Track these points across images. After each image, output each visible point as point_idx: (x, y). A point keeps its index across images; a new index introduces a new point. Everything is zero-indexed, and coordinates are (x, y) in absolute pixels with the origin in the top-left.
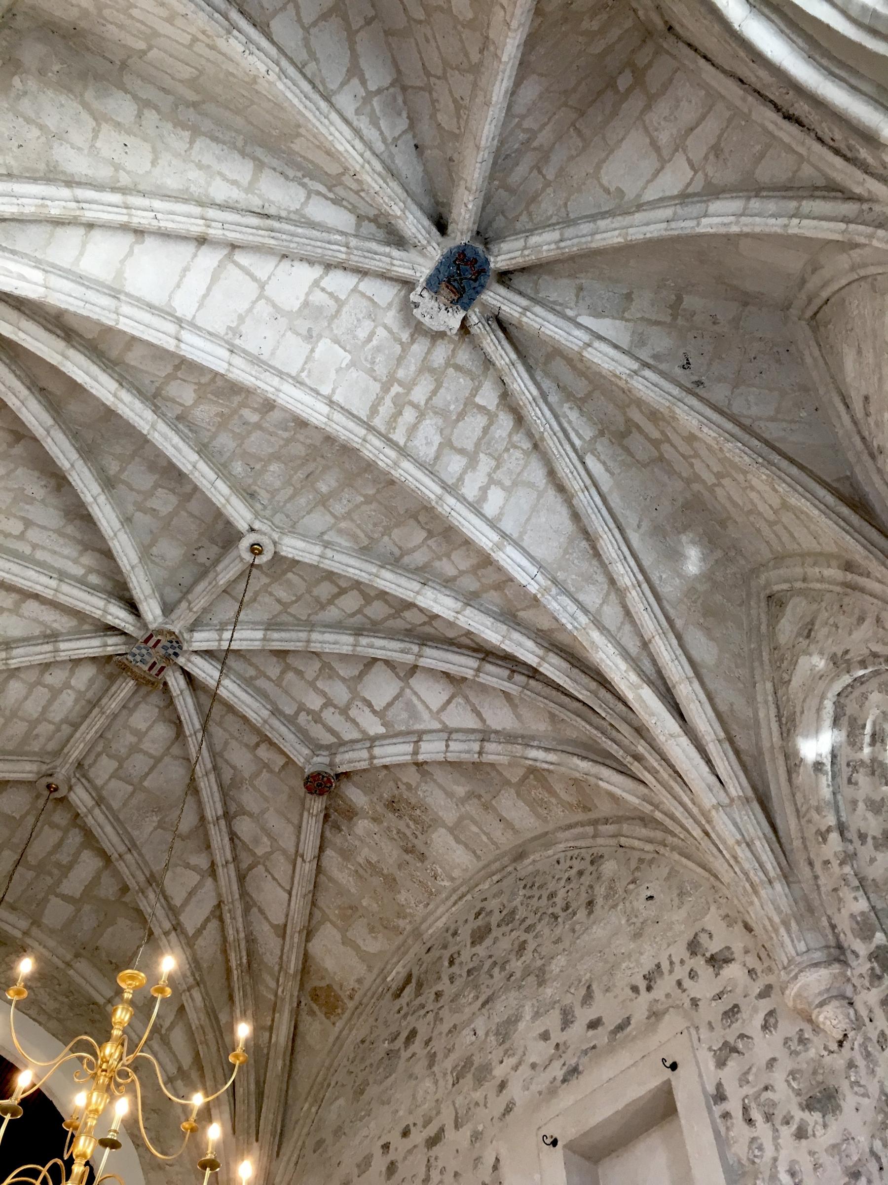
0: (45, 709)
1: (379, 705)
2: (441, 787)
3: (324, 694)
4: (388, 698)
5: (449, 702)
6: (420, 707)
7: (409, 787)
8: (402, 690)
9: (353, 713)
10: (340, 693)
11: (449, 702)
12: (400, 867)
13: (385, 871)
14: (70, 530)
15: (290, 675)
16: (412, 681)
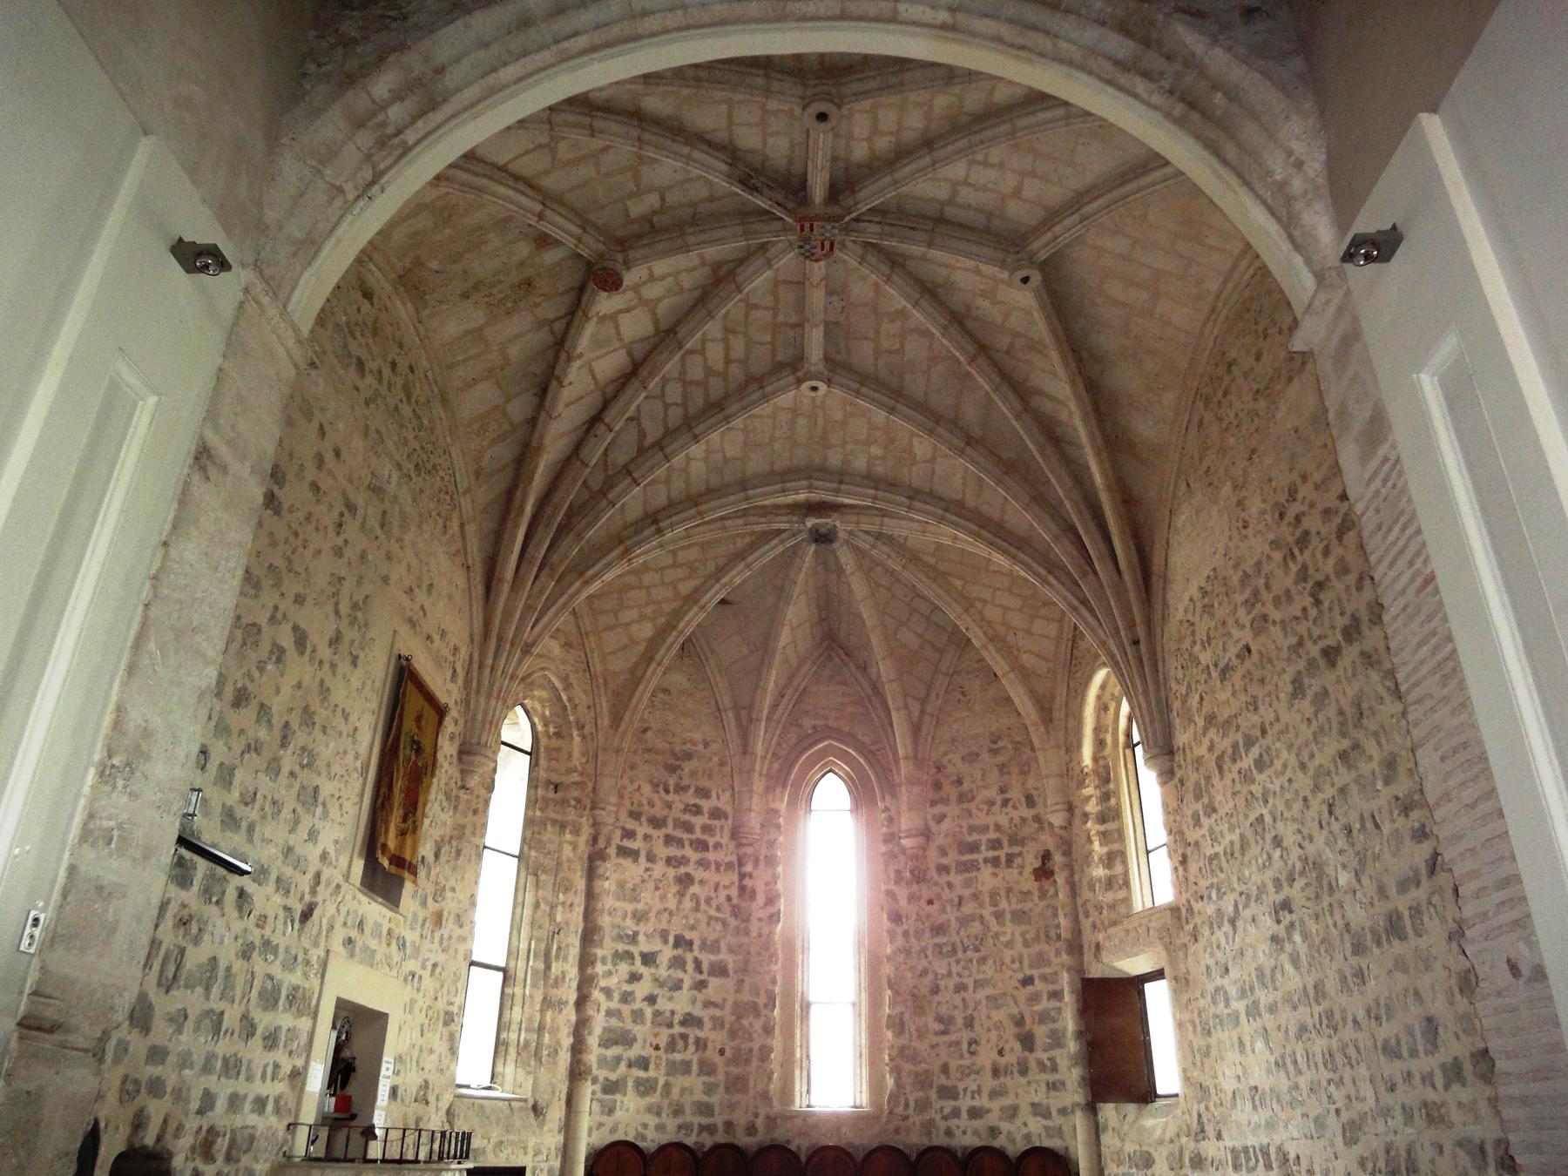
0: (875, 119)
1: (624, 320)
2: (523, 334)
3: (662, 278)
4: (622, 328)
5: (594, 378)
6: (603, 351)
7: (536, 305)
8: (621, 340)
9: (630, 295)
10: (652, 291)
11: (594, 378)
12: (465, 271)
13: (467, 256)
14: (944, 272)
15: (696, 262)
16: (623, 352)
